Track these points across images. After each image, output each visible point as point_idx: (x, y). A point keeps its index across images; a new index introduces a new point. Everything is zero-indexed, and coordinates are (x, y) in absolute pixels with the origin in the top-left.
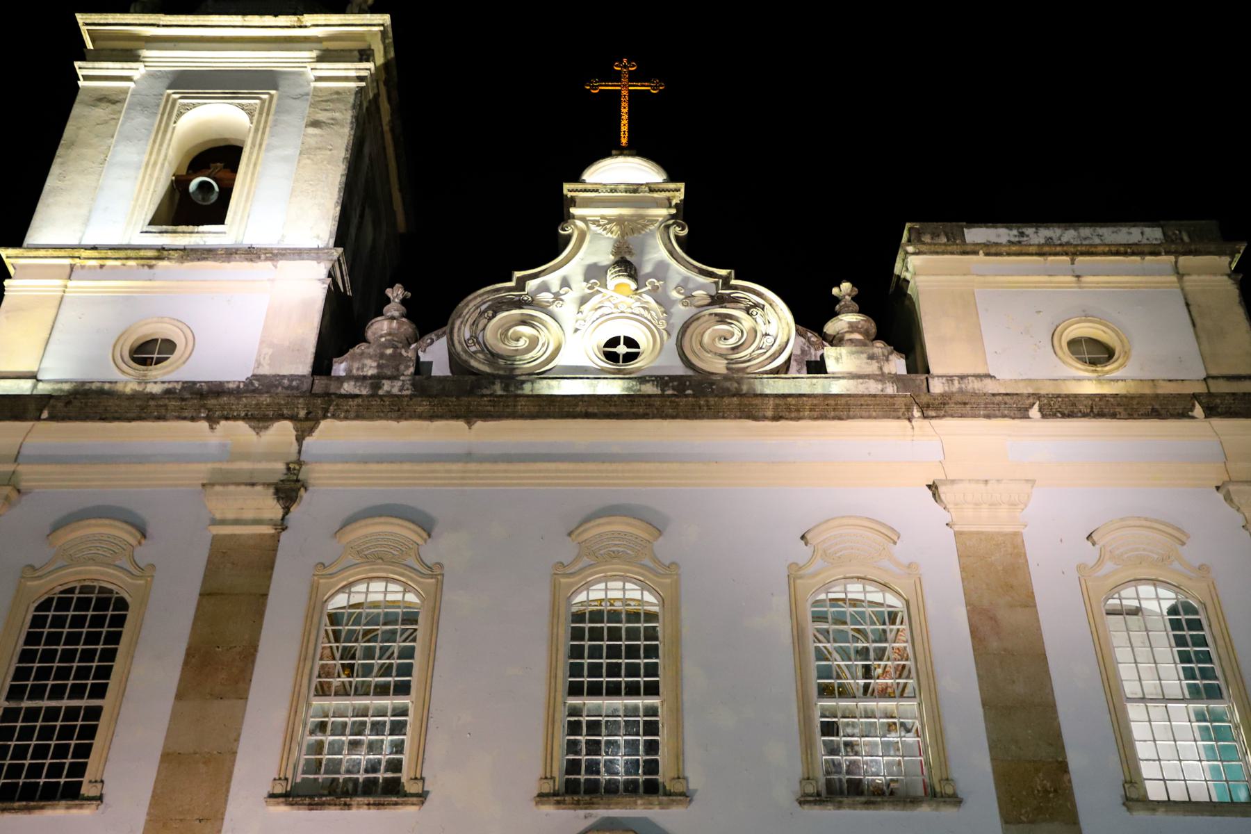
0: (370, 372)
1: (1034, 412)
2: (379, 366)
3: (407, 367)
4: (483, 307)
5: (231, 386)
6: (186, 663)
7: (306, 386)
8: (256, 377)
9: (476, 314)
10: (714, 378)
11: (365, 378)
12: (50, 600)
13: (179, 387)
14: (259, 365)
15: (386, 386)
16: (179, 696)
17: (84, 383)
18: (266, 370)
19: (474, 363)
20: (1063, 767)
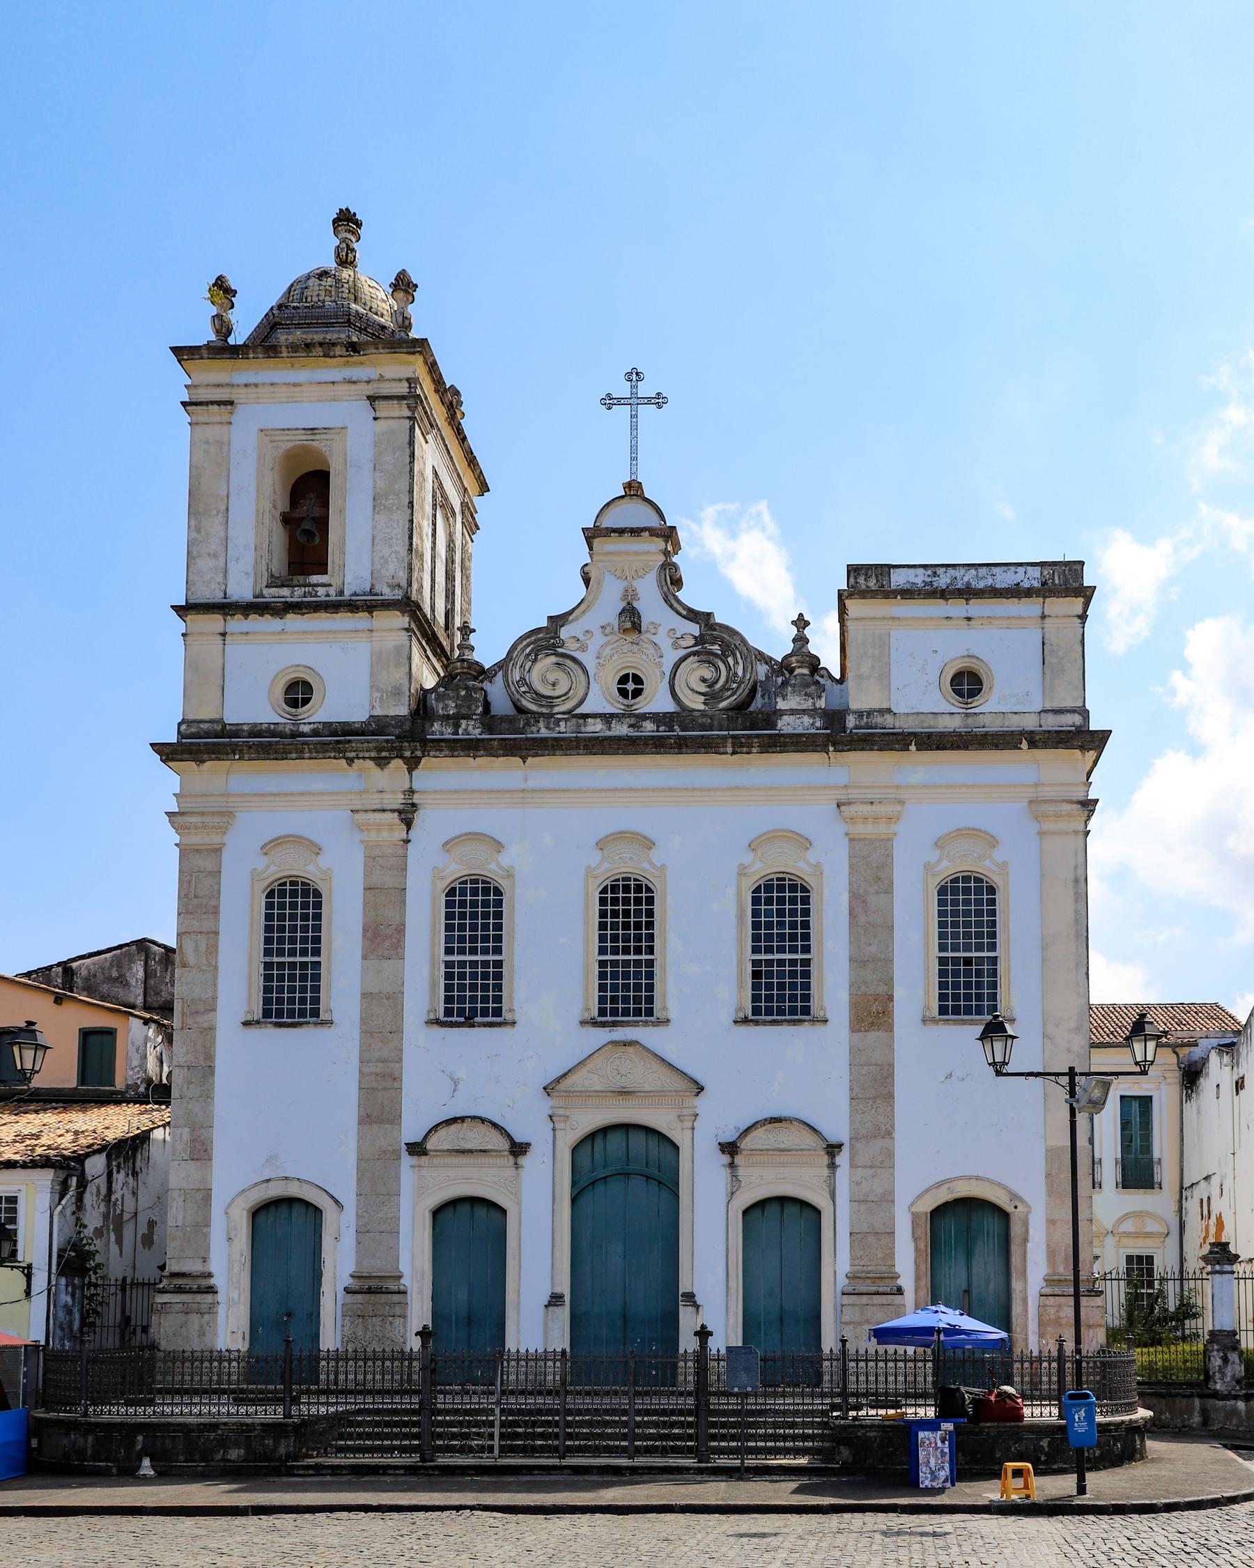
1: (913, 748)
4: (528, 650)
6: (364, 936)
7: (407, 726)
9: (522, 658)
10: (696, 714)
11: (448, 717)
12: (272, 891)
15: (464, 723)
16: (364, 958)
17: (256, 725)
19: (524, 702)
20: (890, 998)
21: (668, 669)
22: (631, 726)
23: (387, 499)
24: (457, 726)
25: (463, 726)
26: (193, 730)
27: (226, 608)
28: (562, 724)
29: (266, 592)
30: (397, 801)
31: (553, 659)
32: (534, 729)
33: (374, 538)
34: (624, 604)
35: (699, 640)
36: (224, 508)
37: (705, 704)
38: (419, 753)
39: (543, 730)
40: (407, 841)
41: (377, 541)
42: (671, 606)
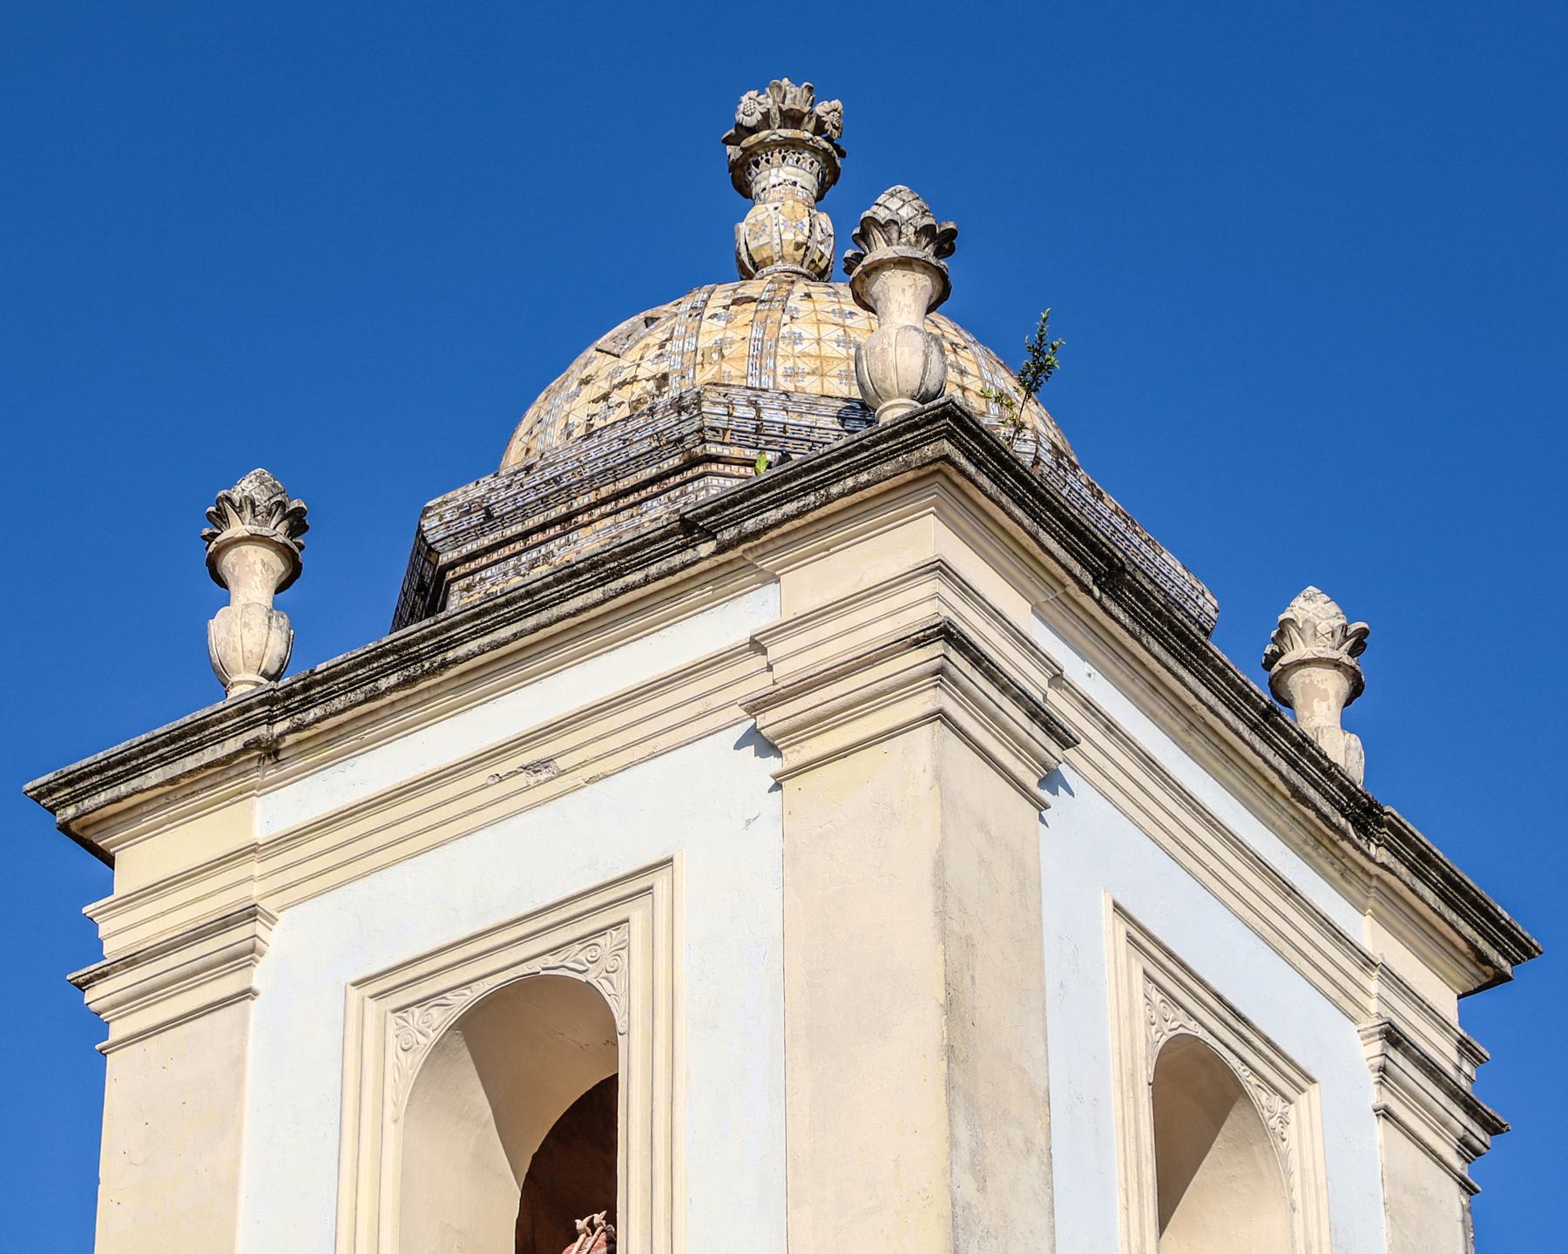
36: (1040, 1139)
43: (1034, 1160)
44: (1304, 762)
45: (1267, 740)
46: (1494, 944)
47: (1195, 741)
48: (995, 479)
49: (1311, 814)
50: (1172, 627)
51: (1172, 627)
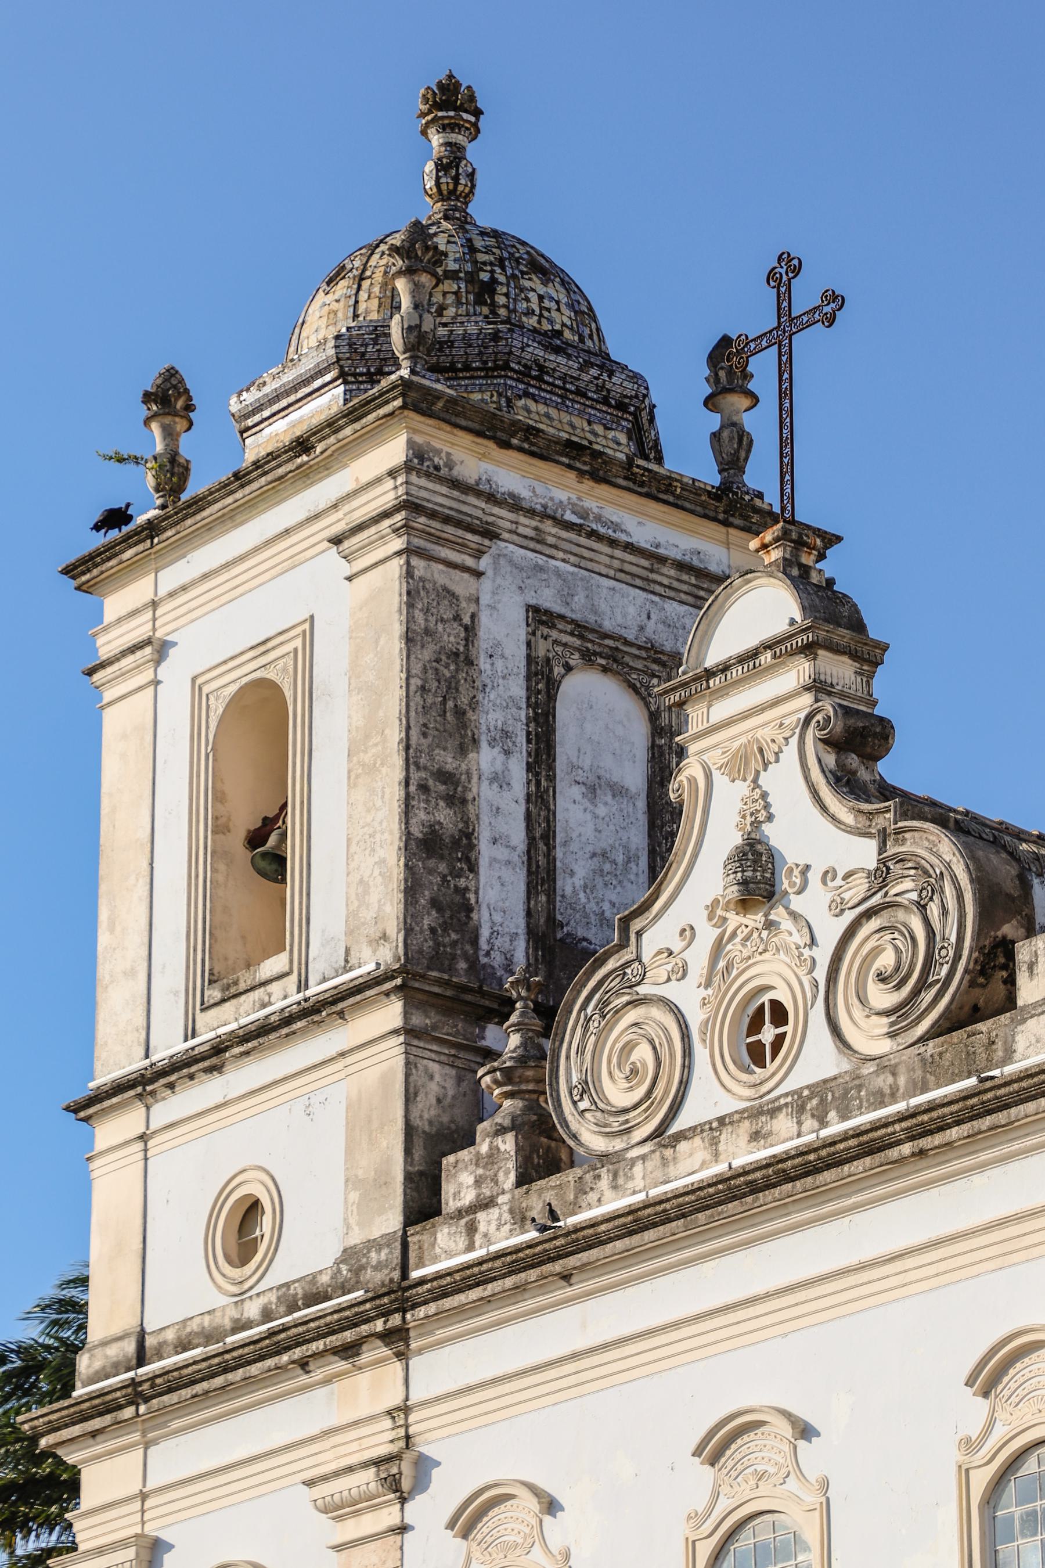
0: (468, 1197)
2: (478, 1182)
3: (507, 1173)
5: (325, 1279)
8: (349, 1255)
11: (460, 1213)
13: (274, 1299)
14: (348, 1227)
18: (356, 1238)
21: (821, 974)
22: (756, 1136)
23: (365, 752)
24: (472, 1229)
25: (482, 1228)
26: (97, 1365)
27: (145, 1084)
28: (638, 1169)
29: (203, 1020)
30: (380, 1440)
31: (632, 1015)
32: (592, 1197)
33: (349, 840)
34: (737, 839)
35: (881, 876)
37: (892, 1035)
38: (396, 1320)
39: (608, 1194)
40: (403, 1529)
41: (354, 848)
42: (824, 808)
43: (141, 881)
44: (267, 467)
45: (250, 482)
46: (387, 402)
47: (239, 519)
48: (96, 566)
49: (291, 475)
50: (184, 509)
51: (184, 509)
